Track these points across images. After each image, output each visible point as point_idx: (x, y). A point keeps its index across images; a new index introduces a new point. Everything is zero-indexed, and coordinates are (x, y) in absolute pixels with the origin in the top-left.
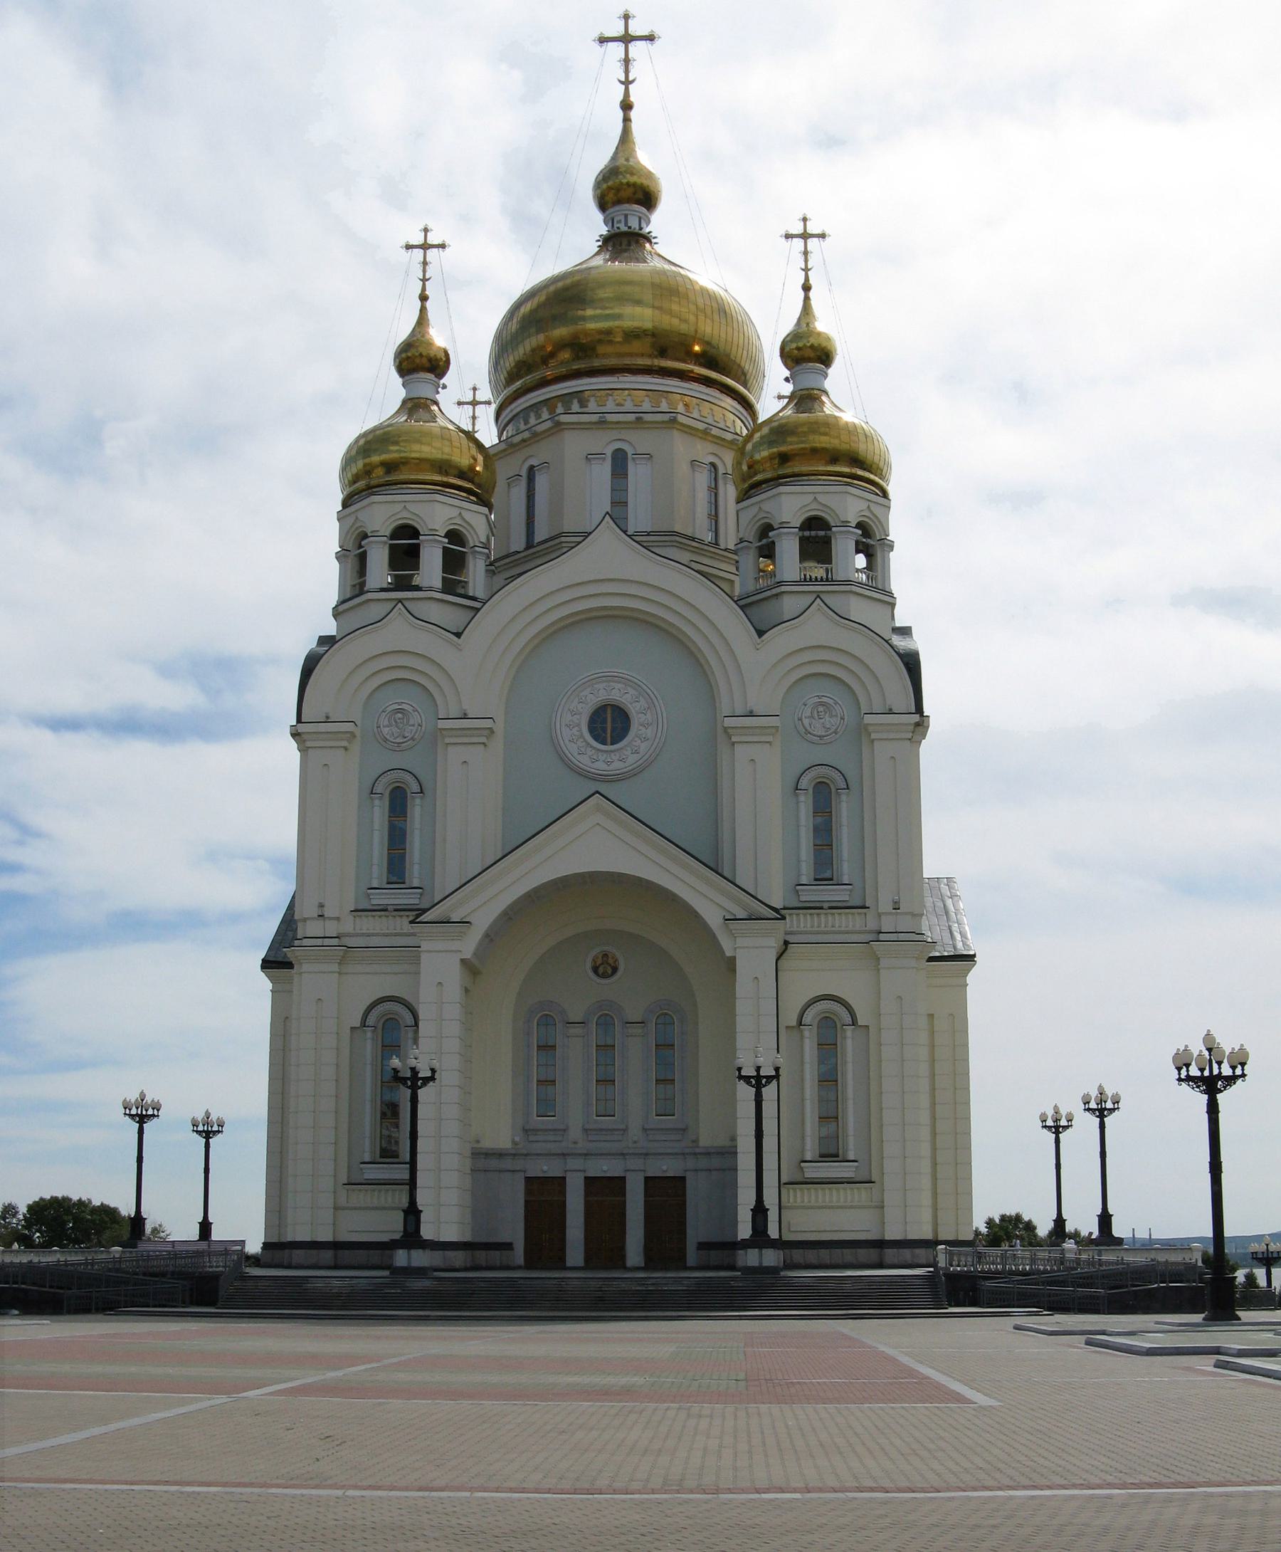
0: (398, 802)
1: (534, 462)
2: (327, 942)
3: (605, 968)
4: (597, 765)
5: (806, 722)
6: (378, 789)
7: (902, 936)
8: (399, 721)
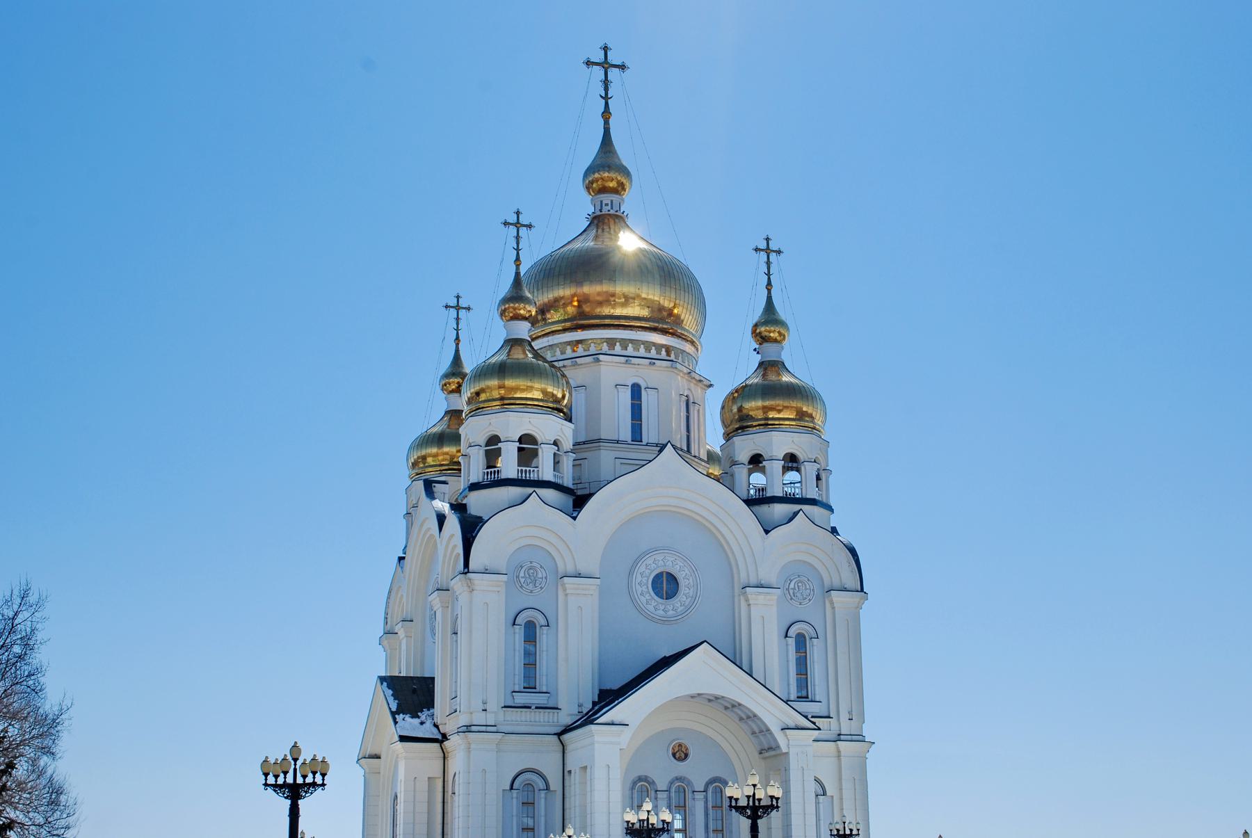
2: (489, 729)
3: (680, 754)
5: (791, 592)
7: (854, 737)
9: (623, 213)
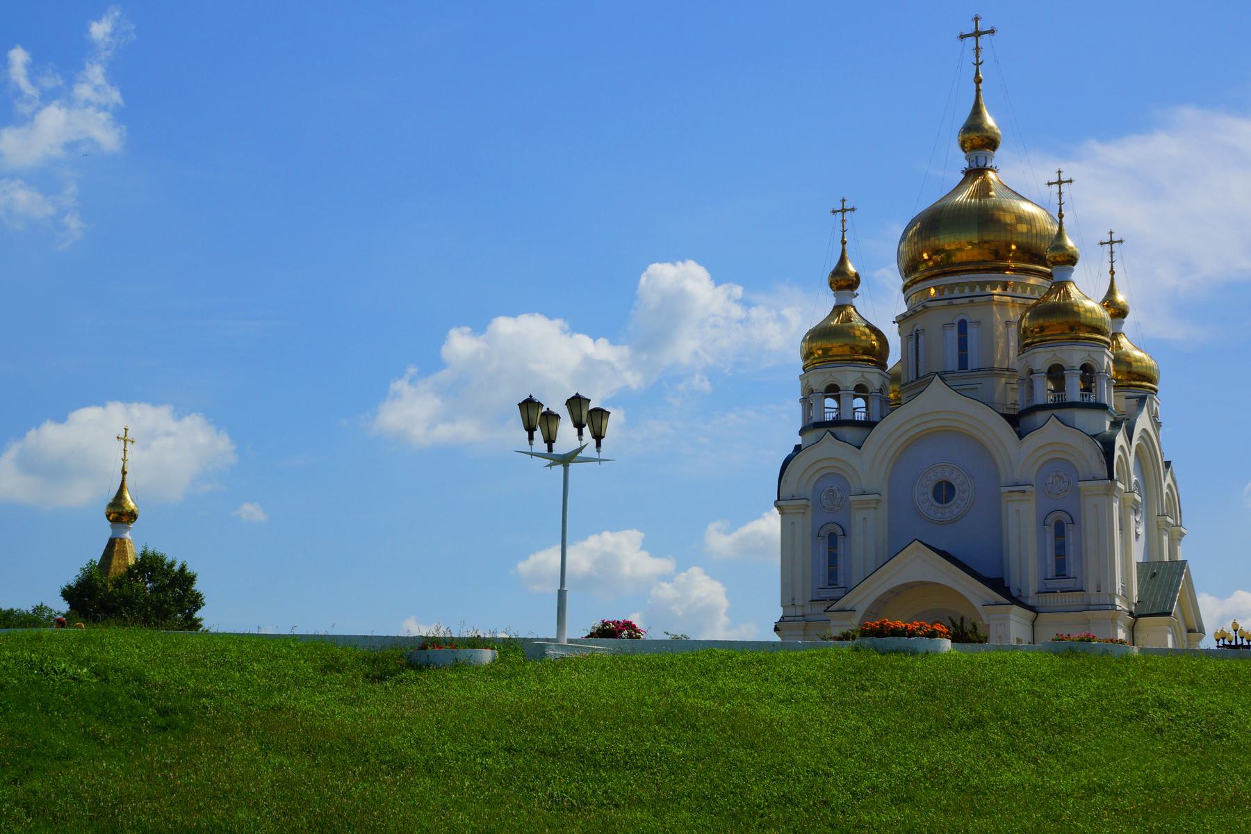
0: (832, 540)
1: (918, 327)
2: (797, 618)
4: (939, 515)
6: (822, 533)
7: (1102, 607)
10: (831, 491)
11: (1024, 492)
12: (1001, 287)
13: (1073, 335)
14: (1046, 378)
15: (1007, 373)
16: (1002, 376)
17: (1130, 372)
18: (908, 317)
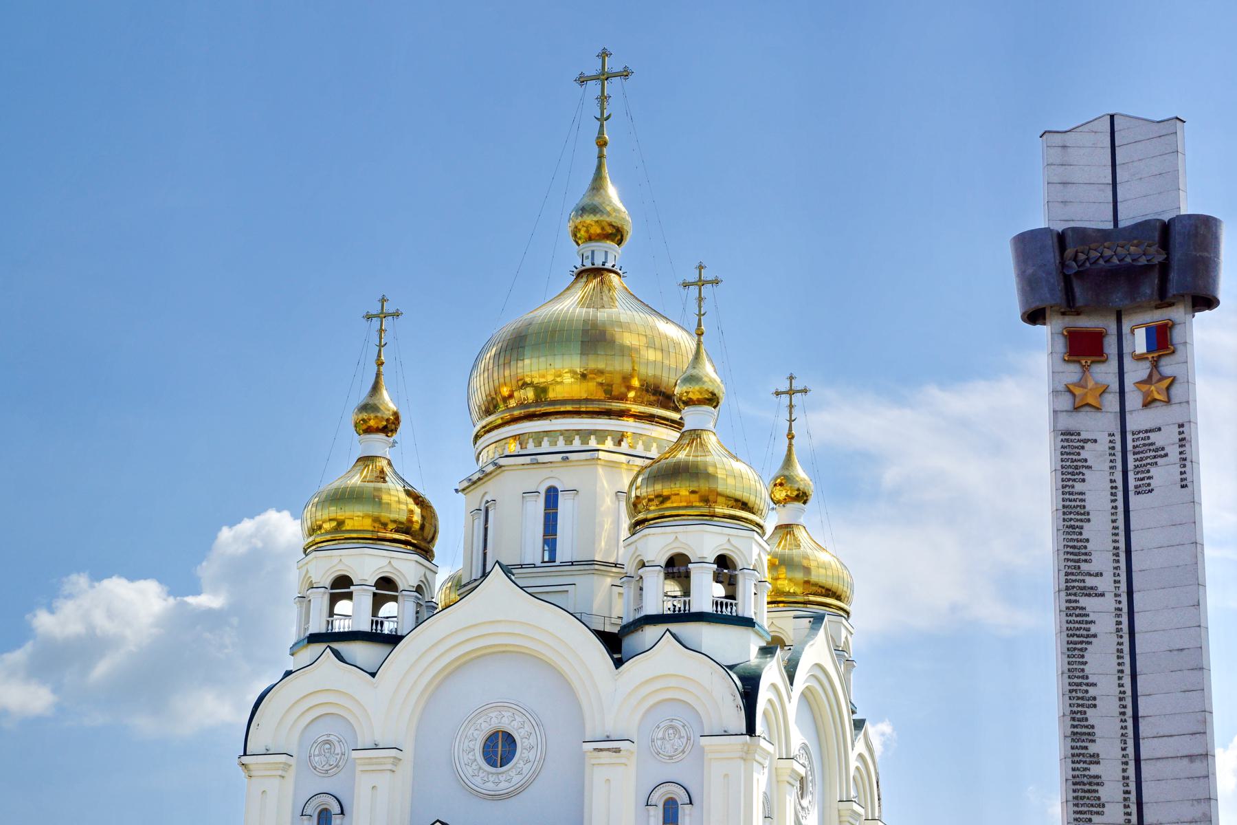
1: (488, 498)
6: (308, 811)
8: (326, 751)
9: (577, 268)
10: (327, 742)
11: (617, 751)
12: (613, 439)
13: (705, 511)
14: (662, 575)
15: (614, 570)
16: (604, 574)
17: (807, 582)
18: (474, 483)
